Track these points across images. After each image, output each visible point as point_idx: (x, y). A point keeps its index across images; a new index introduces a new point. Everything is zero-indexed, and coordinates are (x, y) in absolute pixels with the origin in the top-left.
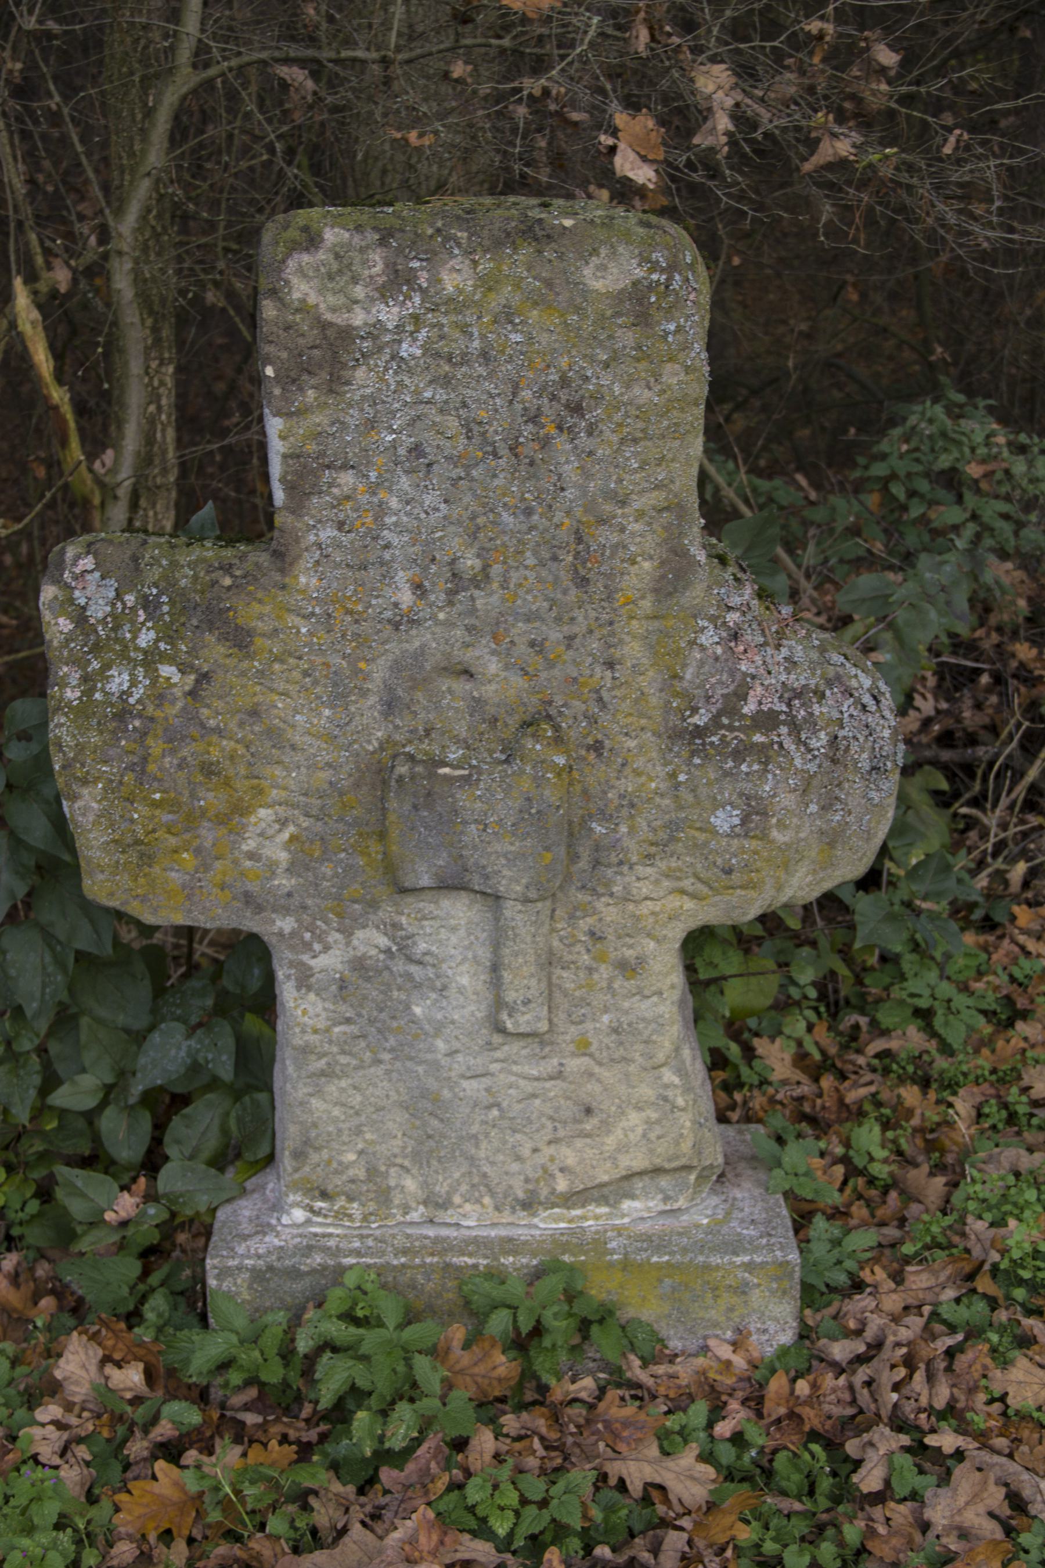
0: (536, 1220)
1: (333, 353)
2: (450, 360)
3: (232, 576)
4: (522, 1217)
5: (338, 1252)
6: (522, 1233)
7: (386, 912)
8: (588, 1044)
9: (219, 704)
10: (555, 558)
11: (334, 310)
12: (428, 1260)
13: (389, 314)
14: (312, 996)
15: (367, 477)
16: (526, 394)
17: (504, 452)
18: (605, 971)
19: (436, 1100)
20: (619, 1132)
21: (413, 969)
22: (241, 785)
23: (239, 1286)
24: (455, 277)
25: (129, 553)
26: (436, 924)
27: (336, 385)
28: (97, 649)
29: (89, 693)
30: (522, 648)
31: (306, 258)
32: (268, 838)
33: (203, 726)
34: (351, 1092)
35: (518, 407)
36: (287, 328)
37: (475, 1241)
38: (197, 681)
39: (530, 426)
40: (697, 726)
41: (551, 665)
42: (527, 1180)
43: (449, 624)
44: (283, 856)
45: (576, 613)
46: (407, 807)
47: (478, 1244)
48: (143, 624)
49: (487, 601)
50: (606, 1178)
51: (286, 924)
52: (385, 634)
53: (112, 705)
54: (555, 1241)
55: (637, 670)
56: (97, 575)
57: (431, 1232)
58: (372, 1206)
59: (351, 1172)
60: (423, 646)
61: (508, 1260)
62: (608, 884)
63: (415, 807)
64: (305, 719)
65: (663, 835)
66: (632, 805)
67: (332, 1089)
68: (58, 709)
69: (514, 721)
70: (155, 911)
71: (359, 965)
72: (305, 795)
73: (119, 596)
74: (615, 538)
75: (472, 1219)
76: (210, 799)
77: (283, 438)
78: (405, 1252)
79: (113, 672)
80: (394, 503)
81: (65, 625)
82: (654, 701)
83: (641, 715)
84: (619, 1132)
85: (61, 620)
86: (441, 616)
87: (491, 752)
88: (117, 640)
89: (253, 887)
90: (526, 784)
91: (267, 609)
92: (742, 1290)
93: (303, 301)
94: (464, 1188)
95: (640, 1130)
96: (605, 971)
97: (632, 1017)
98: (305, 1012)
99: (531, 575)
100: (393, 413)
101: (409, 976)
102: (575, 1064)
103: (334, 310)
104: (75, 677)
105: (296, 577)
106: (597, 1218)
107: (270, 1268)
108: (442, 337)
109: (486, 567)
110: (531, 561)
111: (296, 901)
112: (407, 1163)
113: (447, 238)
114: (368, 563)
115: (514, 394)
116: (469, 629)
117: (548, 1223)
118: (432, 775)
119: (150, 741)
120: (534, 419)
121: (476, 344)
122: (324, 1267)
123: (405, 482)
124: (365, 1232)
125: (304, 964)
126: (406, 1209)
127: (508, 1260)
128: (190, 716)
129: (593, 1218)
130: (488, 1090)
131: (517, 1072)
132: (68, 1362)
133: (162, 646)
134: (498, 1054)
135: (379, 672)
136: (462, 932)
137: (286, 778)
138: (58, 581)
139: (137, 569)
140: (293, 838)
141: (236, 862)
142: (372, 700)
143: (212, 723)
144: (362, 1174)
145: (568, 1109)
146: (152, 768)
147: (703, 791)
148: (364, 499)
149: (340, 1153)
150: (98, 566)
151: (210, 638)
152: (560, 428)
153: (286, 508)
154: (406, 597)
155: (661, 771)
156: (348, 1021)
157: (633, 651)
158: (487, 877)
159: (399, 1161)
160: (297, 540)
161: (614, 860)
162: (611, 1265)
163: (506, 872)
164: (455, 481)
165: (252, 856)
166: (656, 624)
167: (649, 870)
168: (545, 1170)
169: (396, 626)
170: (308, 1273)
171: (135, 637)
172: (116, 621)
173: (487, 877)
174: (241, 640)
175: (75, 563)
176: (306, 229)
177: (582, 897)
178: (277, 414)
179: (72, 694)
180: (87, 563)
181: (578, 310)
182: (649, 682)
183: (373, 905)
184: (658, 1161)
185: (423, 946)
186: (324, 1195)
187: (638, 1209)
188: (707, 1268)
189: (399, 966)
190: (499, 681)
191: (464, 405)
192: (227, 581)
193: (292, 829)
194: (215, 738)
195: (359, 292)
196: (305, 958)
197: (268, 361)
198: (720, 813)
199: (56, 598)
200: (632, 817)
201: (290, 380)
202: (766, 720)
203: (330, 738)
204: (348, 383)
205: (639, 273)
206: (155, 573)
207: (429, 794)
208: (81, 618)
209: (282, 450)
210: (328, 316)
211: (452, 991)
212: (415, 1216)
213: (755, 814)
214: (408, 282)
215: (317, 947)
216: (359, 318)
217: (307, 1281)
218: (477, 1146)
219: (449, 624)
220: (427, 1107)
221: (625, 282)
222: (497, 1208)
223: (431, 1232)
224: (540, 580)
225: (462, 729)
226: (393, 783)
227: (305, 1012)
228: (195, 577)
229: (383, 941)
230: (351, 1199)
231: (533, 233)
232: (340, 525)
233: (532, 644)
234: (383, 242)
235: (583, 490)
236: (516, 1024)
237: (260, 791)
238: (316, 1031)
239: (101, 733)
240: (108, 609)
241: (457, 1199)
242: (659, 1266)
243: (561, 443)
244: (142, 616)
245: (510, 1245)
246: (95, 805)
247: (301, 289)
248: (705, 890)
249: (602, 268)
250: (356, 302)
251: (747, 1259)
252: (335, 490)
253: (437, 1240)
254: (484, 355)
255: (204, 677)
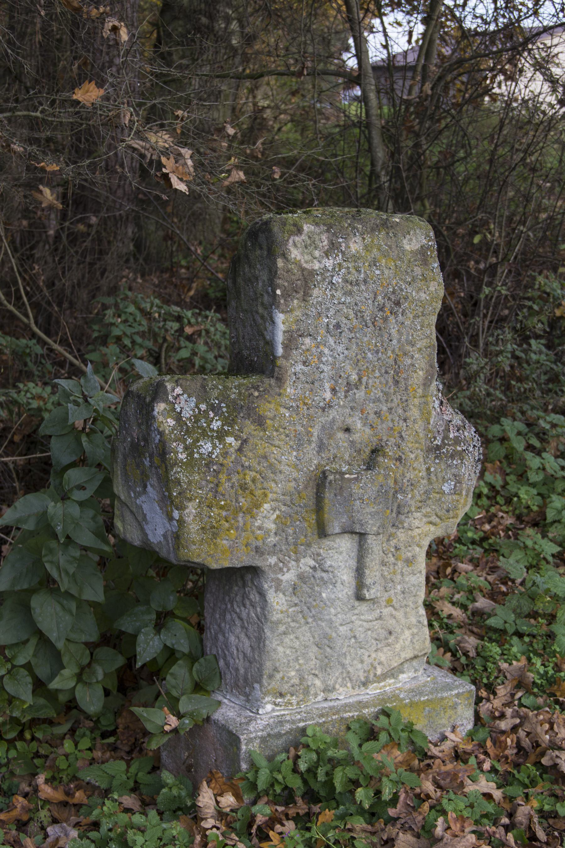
0: (368, 691)
2: (351, 284)
3: (258, 391)
4: (363, 690)
5: (293, 722)
6: (364, 698)
7: (314, 548)
8: (392, 601)
9: (250, 454)
10: (386, 372)
11: (306, 262)
12: (334, 717)
13: (329, 263)
14: (281, 595)
15: (316, 339)
16: (380, 298)
17: (370, 324)
18: (400, 564)
19: (330, 639)
20: (401, 641)
21: (324, 575)
22: (258, 493)
23: (255, 746)
24: (355, 246)
25: (199, 384)
26: (334, 551)
27: (306, 296)
28: (188, 432)
29: (191, 454)
30: (372, 416)
31: (297, 239)
32: (267, 518)
33: (243, 466)
34: (295, 640)
35: (376, 303)
36: (288, 271)
37: (346, 705)
38: (242, 444)
39: (381, 313)
40: (437, 445)
41: (382, 422)
42: (365, 671)
43: (344, 407)
44: (272, 526)
45: (394, 397)
46: (332, 495)
47: (347, 707)
48: (213, 419)
49: (360, 394)
50: (396, 664)
51: (272, 560)
52: (319, 413)
53: (204, 459)
54: (378, 699)
55: (415, 421)
56: (185, 396)
57: (325, 705)
58: (301, 697)
59: (292, 681)
60: (334, 418)
61: (366, 711)
62: (402, 522)
63: (335, 495)
65: (424, 497)
66: (412, 485)
67: (287, 640)
68: (176, 464)
69: (368, 451)
70: (217, 561)
71: (301, 577)
72: (283, 495)
73: (197, 406)
74: (409, 361)
75: (345, 695)
77: (283, 323)
78: (322, 716)
79: (201, 443)
80: (326, 351)
81: (171, 422)
82: (421, 435)
83: (417, 442)
84: (401, 641)
85: (169, 420)
86: (342, 403)
87: (359, 466)
88: (198, 427)
89: (260, 543)
90: (381, 478)
91: (272, 406)
92: (454, 707)
93: (295, 258)
94: (340, 680)
95: (409, 639)
96: (400, 564)
97: (409, 585)
98: (278, 603)
99: (378, 381)
100: (328, 309)
101: (322, 578)
102: (387, 611)
103: (306, 262)
104: (180, 448)
105: (285, 390)
106: (390, 685)
107: (269, 735)
108: (349, 273)
109: (360, 379)
110: (377, 374)
111: (278, 548)
112: (317, 672)
113: (354, 228)
115: (375, 298)
116: (352, 408)
117: (373, 691)
118: (343, 479)
119: (221, 476)
120: (381, 309)
121: (362, 276)
122: (291, 730)
123: (331, 341)
124: (298, 710)
125: (278, 579)
126: (316, 695)
127: (366, 711)
128: (236, 462)
129: (389, 686)
130: (351, 630)
132: (204, 797)
133: (226, 428)
134: (356, 612)
135: (315, 431)
136: (344, 554)
137: (277, 488)
138: (166, 401)
139: (205, 391)
140: (278, 517)
141: (253, 532)
142: (313, 445)
143: (247, 464)
144: (297, 681)
145: (383, 633)
146: (221, 489)
147: (439, 475)
148: (314, 350)
149: (288, 672)
150: (184, 391)
151: (248, 422)
152: (391, 313)
153: (283, 356)
154: (328, 395)
155: (424, 467)
156: (296, 605)
157: (414, 413)
158: (362, 525)
159: (313, 672)
160: (287, 372)
161: (406, 511)
162: (406, 705)
163: (370, 522)
164: (350, 340)
165: (260, 528)
166: (423, 400)
167: (419, 514)
168: (372, 665)
169: (323, 409)
170: (284, 734)
171: (209, 426)
172: (197, 418)
173: (362, 525)
174: (260, 422)
175: (173, 390)
176: (295, 225)
177: (393, 530)
178: (282, 312)
179: (182, 456)
180: (178, 390)
181: (400, 259)
182: (419, 426)
183: (309, 545)
184: (416, 653)
185: (329, 563)
186: (281, 695)
188: (442, 699)
189: (319, 574)
190: (362, 433)
191: (356, 304)
192: (256, 394)
193: (278, 512)
194: (247, 471)
195: (317, 253)
196: (280, 576)
197: (278, 287)
198: (446, 484)
199: (165, 409)
200: (412, 490)
201: (287, 295)
203: (296, 466)
204: (311, 296)
205: (424, 241)
206: (216, 393)
207: (341, 488)
208: (178, 417)
209: (284, 329)
210: (305, 265)
211: (338, 585)
212: (319, 698)
214: (337, 248)
215: (285, 570)
216: (317, 266)
217: (284, 737)
218: (346, 658)
219: (344, 407)
221: (418, 246)
222: (353, 688)
223: (325, 705)
224: (380, 383)
225: (347, 457)
226: (327, 484)
227: (278, 603)
228: (240, 393)
229: (312, 563)
230: (292, 695)
231: (385, 225)
232: (304, 363)
233: (376, 413)
234: (328, 231)
235: (399, 341)
236: (370, 595)
237: (266, 495)
238: (282, 612)
239: (199, 474)
240: (191, 412)
241: (337, 686)
242: (424, 702)
243: (392, 319)
244: (212, 414)
245: (361, 705)
246: (194, 511)
247: (295, 254)
248: (438, 520)
249: (411, 240)
250: (315, 258)
251: (456, 692)
252: (303, 347)
253: (331, 708)
254: (365, 281)
255: (245, 441)
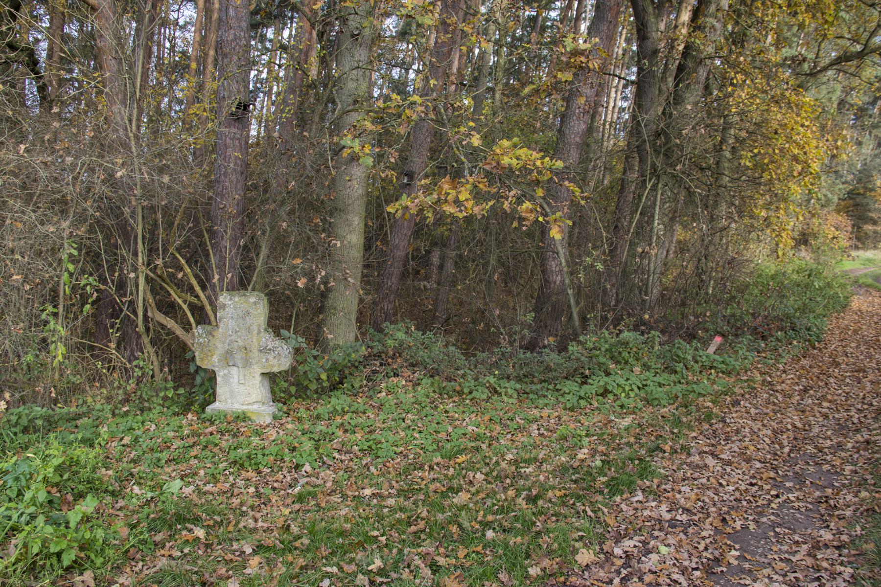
1: (224, 306)
24: (237, 299)
32: (215, 359)
49: (239, 334)
64: (220, 345)
76: (210, 354)
114: (227, 329)
117: (245, 407)
129: (250, 407)
131: (241, 388)
137: (218, 352)
174: (213, 336)
187: (255, 407)
190: (241, 343)
202: (270, 350)
213: (267, 360)
220: (231, 392)
231: (244, 295)
